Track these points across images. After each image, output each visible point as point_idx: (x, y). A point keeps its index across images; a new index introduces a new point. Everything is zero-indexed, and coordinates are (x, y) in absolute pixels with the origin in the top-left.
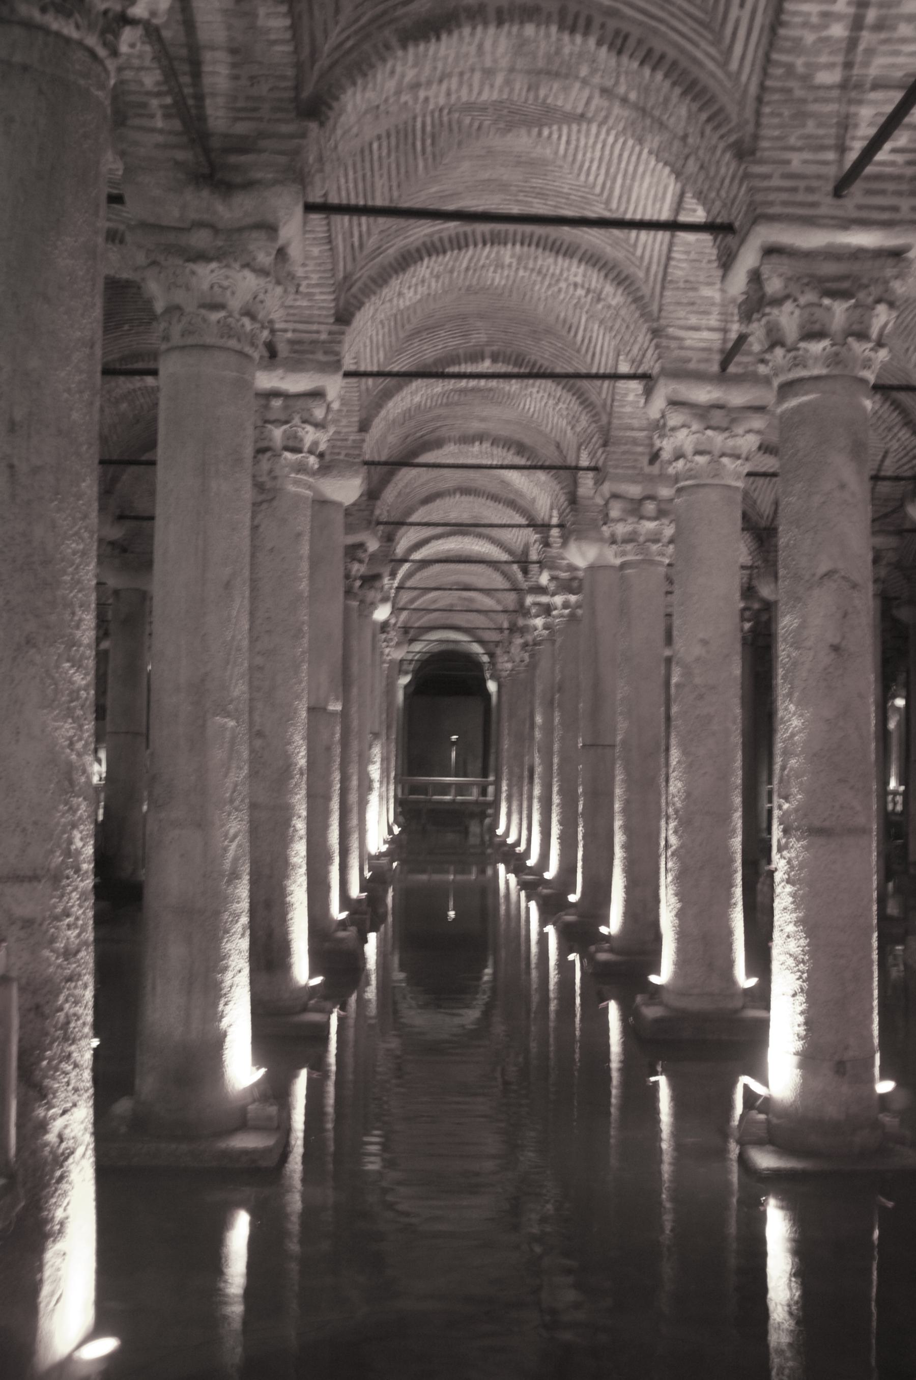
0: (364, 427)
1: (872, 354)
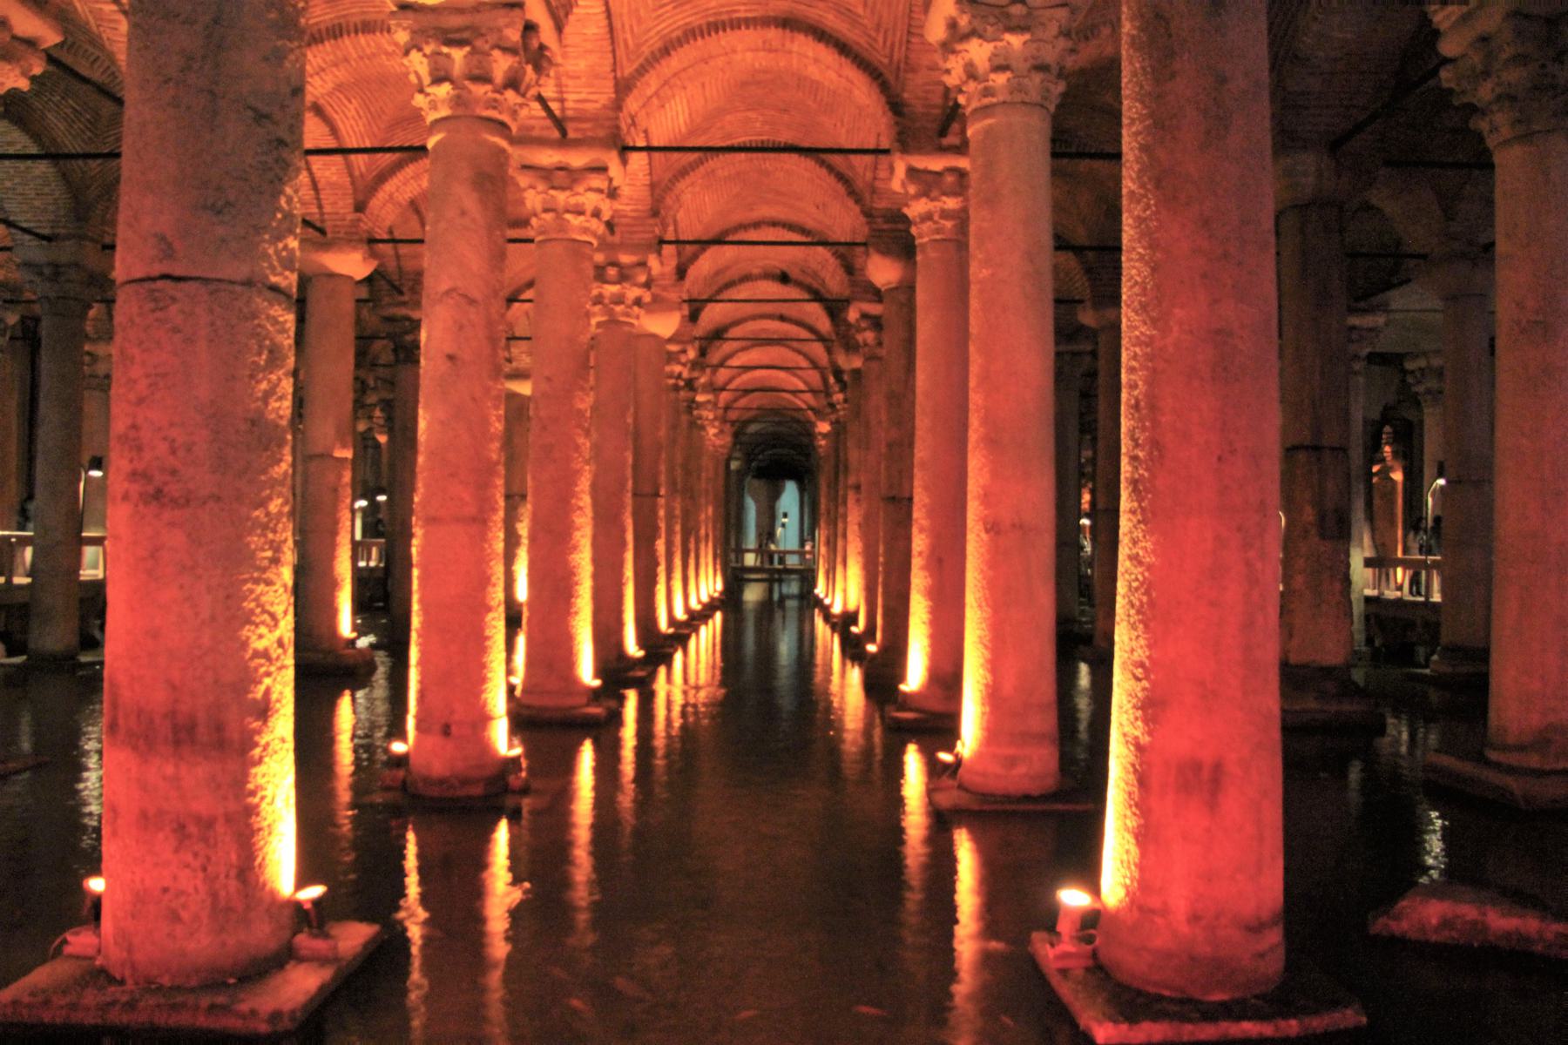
0: (360, 207)
1: (498, 96)
